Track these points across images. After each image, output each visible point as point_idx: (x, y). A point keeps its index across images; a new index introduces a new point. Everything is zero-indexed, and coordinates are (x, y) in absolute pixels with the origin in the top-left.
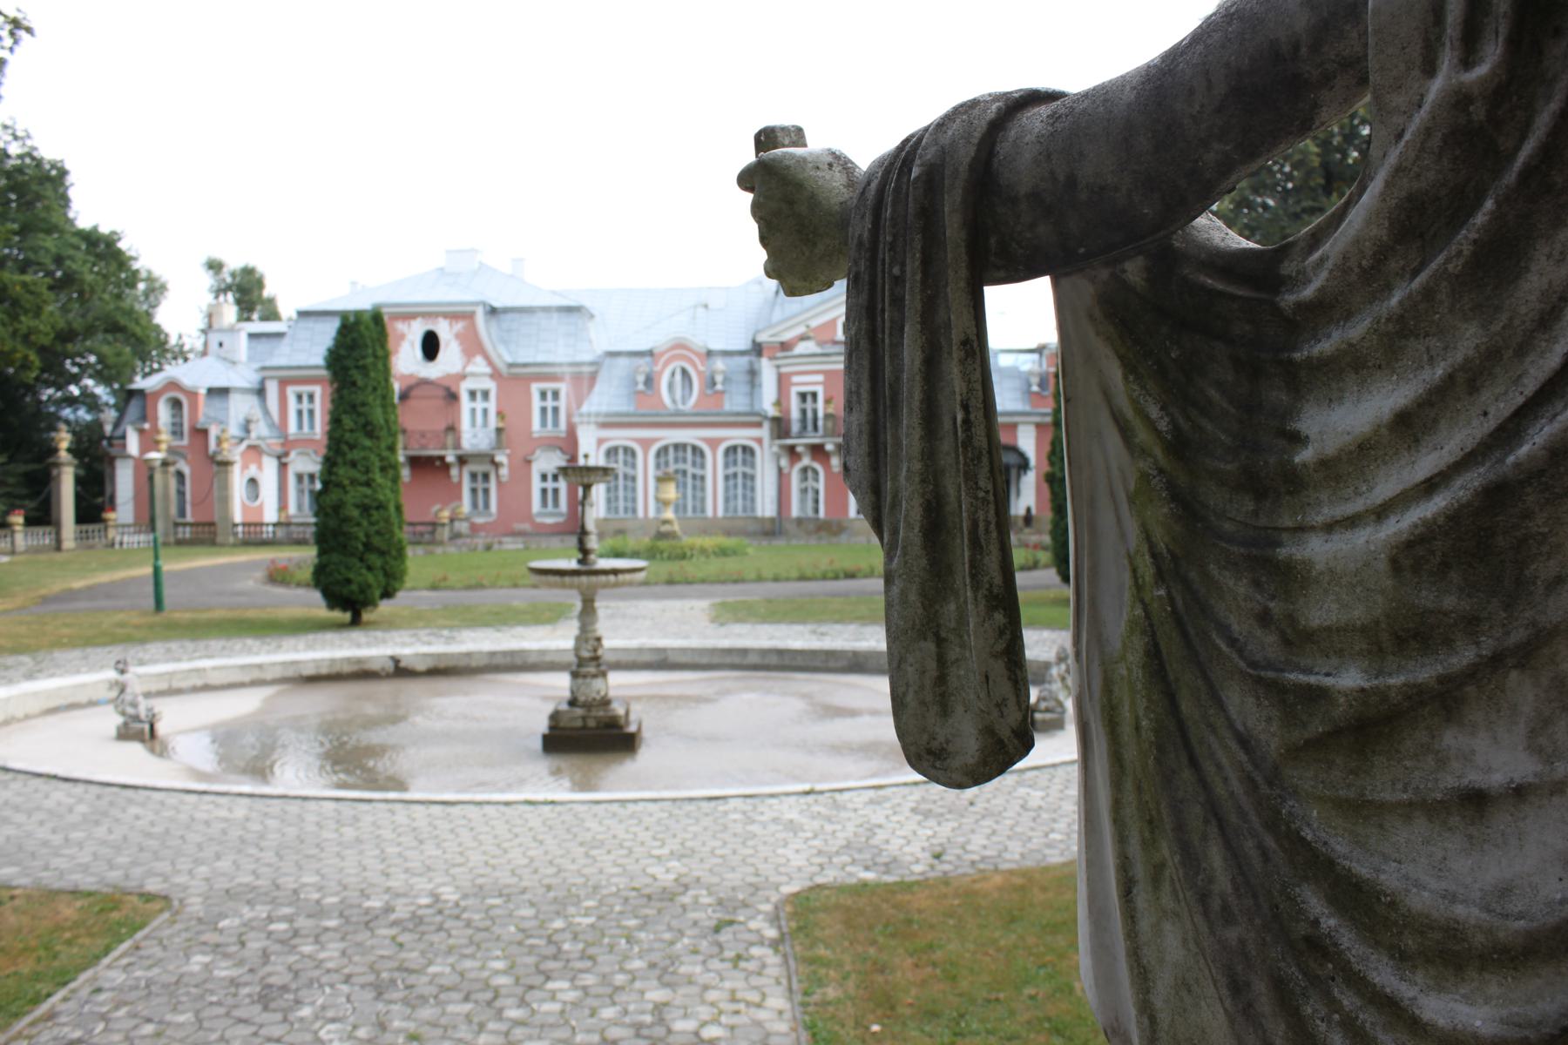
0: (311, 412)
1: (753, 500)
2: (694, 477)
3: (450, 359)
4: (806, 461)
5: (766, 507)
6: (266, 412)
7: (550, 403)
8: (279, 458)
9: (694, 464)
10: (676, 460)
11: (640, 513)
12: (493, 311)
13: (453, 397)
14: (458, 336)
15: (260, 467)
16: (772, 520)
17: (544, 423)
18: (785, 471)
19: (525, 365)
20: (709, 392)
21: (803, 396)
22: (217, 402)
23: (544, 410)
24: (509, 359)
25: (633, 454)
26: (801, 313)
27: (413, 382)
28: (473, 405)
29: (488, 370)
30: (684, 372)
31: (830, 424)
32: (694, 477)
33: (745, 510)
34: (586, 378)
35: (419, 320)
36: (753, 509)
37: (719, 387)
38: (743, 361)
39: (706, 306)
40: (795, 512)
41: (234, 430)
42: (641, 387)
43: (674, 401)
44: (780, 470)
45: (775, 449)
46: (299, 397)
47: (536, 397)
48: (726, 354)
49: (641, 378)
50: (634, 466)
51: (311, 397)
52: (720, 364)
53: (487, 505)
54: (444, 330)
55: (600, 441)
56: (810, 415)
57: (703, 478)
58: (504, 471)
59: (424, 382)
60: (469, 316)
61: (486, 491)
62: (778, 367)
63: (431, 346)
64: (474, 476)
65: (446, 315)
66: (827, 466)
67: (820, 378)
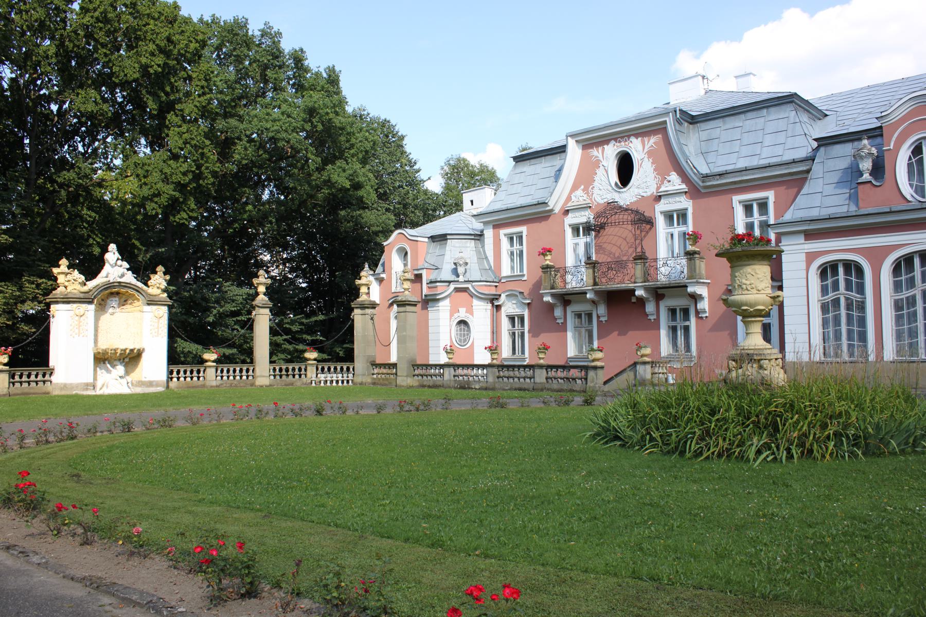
0: (521, 252)
6: (482, 257)
11: (872, 358)
13: (643, 221)
14: (650, 154)
15: (470, 311)
19: (721, 175)
22: (435, 248)
24: (704, 170)
25: (860, 271)
28: (671, 230)
41: (446, 274)
42: (866, 176)
47: (739, 211)
49: (866, 165)
50: (861, 289)
51: (521, 238)
54: (637, 148)
55: (811, 257)
58: (704, 305)
59: (613, 208)
61: (687, 329)
64: (673, 312)
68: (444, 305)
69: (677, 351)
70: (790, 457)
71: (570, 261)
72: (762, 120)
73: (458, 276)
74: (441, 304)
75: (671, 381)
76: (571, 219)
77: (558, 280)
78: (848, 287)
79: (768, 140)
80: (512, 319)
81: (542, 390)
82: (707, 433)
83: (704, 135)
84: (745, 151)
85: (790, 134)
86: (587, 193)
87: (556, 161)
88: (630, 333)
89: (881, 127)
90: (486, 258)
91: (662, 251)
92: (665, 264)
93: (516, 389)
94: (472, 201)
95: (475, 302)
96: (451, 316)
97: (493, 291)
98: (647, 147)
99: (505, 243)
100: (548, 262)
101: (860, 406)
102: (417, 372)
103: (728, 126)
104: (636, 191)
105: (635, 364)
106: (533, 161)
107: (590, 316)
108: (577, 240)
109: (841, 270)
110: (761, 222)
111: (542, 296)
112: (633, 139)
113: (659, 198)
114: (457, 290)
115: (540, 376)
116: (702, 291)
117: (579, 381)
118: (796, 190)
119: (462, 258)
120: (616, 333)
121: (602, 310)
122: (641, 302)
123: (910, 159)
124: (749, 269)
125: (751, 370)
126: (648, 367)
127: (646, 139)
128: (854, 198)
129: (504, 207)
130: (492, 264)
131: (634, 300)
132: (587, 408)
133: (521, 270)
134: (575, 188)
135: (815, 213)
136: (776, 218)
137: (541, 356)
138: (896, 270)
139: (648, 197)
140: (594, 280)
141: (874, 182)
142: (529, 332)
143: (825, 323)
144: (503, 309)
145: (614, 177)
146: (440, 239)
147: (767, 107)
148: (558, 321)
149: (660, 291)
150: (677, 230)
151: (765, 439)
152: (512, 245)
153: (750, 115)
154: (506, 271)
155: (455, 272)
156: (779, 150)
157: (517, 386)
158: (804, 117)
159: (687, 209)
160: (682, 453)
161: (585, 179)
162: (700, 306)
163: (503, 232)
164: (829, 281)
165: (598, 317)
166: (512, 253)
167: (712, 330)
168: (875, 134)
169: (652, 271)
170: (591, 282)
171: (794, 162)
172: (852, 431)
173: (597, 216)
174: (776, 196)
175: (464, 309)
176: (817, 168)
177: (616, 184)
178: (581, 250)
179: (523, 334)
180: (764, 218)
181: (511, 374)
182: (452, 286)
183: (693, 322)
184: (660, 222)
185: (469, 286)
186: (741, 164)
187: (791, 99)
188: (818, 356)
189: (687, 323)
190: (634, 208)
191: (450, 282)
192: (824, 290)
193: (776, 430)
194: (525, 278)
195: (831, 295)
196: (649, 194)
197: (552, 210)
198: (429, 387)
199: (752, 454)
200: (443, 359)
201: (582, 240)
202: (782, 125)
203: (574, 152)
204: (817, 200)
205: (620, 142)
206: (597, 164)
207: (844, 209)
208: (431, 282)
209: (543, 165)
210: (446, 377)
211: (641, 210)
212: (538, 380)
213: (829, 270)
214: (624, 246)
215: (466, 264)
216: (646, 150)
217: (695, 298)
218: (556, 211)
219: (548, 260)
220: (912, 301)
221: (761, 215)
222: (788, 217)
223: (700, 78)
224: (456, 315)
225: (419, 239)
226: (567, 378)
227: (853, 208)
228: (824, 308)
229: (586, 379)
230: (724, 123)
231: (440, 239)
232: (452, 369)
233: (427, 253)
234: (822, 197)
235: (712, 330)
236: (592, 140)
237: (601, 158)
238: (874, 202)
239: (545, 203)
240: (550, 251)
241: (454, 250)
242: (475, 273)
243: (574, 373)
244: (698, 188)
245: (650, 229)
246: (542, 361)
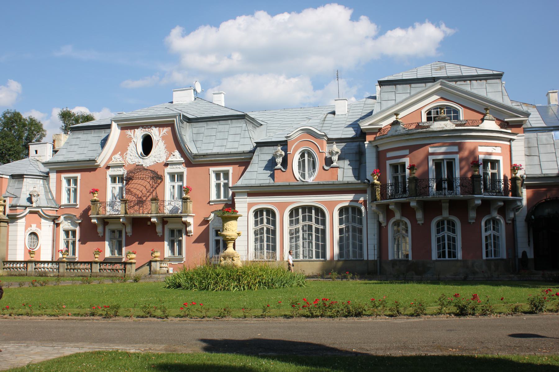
0: (75, 190)
1: (361, 248)
2: (317, 230)
3: (160, 152)
4: (398, 216)
5: (370, 253)
7: (222, 181)
8: (53, 221)
9: (317, 222)
10: (304, 219)
11: (278, 259)
12: (190, 121)
13: (158, 178)
14: (163, 138)
15: (39, 226)
16: (374, 261)
17: (218, 195)
18: (383, 225)
19: (204, 155)
20: (326, 168)
21: (395, 167)
22: (15, 183)
23: (218, 186)
24: (194, 151)
26: (392, 107)
27: (131, 168)
29: (182, 159)
30: (310, 154)
31: (413, 186)
32: (317, 230)
33: (354, 252)
34: (243, 161)
35: (139, 130)
36: (361, 255)
37: (335, 164)
38: (354, 145)
39: (334, 113)
40: (390, 258)
42: (279, 166)
43: (303, 175)
44: (380, 224)
45: (374, 208)
46: (69, 181)
47: (213, 176)
48: (339, 141)
49: (279, 160)
50: (274, 224)
52: (336, 148)
53: (180, 253)
54: (155, 133)
55: (250, 205)
56: (400, 180)
57: (324, 231)
58: (190, 228)
59: (140, 168)
60: (171, 125)
61: (180, 242)
62: (377, 147)
63: (148, 145)
65: (156, 126)
66: (414, 221)
67: (406, 152)
68: (21, 222)
69: (174, 254)
70: (244, 289)
71: (109, 198)
72: (228, 126)
73: (32, 203)
74: (19, 221)
75: (171, 271)
76: (111, 172)
77: (101, 209)
78: (268, 223)
79: (231, 138)
80: (67, 232)
81: (96, 276)
82: (216, 283)
83: (195, 130)
84: (218, 143)
85: (242, 136)
86: (123, 157)
87: (103, 134)
88: (146, 243)
89: (286, 141)
90: (50, 192)
91: (168, 197)
92: (170, 204)
93: (79, 276)
94: (36, 151)
95: (43, 221)
96: (26, 229)
97: (54, 214)
98: (161, 134)
99: (64, 183)
100: (95, 198)
101: (267, 273)
102: (6, 266)
103: (209, 127)
104: (154, 159)
105: (151, 262)
106: (85, 131)
107: (120, 232)
108: (114, 185)
109: (265, 213)
110: (224, 183)
111: (91, 219)
112: (154, 129)
113: (166, 165)
114: (31, 212)
115: (96, 268)
116: (190, 220)
117: (120, 271)
118: (244, 167)
119: (35, 191)
120: (137, 243)
121: (129, 229)
122: (154, 224)
123: (299, 159)
124: (229, 223)
125: (229, 261)
126: (158, 263)
127: (161, 129)
128: (272, 176)
129: (66, 160)
130: (55, 196)
131: (149, 223)
132: (135, 284)
133: (75, 200)
134: (114, 153)
135: (253, 183)
136: (232, 184)
137: (97, 256)
138: (291, 215)
139: (160, 163)
140: (126, 211)
141: (283, 169)
142: (79, 241)
143: (256, 240)
144: (61, 225)
145: (140, 150)
146: (20, 177)
147: (231, 119)
148: (99, 235)
149: (165, 219)
150: (177, 184)
151: (236, 283)
152: (69, 184)
153: (222, 122)
154: (64, 201)
155: (30, 200)
156: (236, 145)
157: (80, 274)
158: (250, 127)
159: (183, 173)
160: (208, 289)
161: (122, 148)
162: (188, 229)
163: (63, 176)
164: (259, 219)
165: (126, 233)
166: (69, 190)
167: (195, 242)
168: (284, 144)
169: (161, 208)
170: (123, 211)
171: (244, 153)
172: (264, 281)
173: (129, 172)
174: (233, 170)
175: (35, 225)
176: (255, 158)
177: (141, 154)
178: (117, 192)
179: (74, 243)
180: (226, 181)
181: (72, 267)
182: (28, 210)
183: (184, 238)
184: (167, 178)
185: (39, 210)
186: (216, 150)
187: (242, 117)
188: (251, 257)
189: (180, 238)
190: (153, 169)
191: (26, 207)
192: (256, 223)
193: (239, 281)
194: (78, 207)
195: (260, 226)
196: (161, 161)
197: (99, 165)
198: (16, 275)
199: (232, 289)
200: (21, 258)
201: (118, 185)
202: (238, 130)
203: (115, 131)
204: (254, 175)
205: (145, 128)
206: (130, 140)
207: (268, 182)
208: (12, 206)
209: (92, 135)
210: (29, 268)
211: (156, 171)
212: (94, 270)
213: (258, 213)
214: (144, 191)
215: (38, 195)
216: (161, 136)
217: (186, 224)
218: (102, 166)
219: (96, 197)
220: (297, 231)
221: (225, 179)
222: (240, 183)
223: (192, 90)
224: (29, 229)
225: (4, 176)
226: (113, 269)
227: (272, 181)
228: (256, 233)
229: (125, 270)
230: (207, 125)
231: (20, 177)
232: (34, 264)
233: (8, 186)
234: (257, 175)
235: (195, 242)
236: (127, 126)
237: (133, 137)
238: (282, 179)
239: (94, 161)
240: (97, 191)
241: (30, 186)
242: (44, 203)
243: (118, 266)
244: (191, 161)
245: (161, 182)
246: (97, 259)
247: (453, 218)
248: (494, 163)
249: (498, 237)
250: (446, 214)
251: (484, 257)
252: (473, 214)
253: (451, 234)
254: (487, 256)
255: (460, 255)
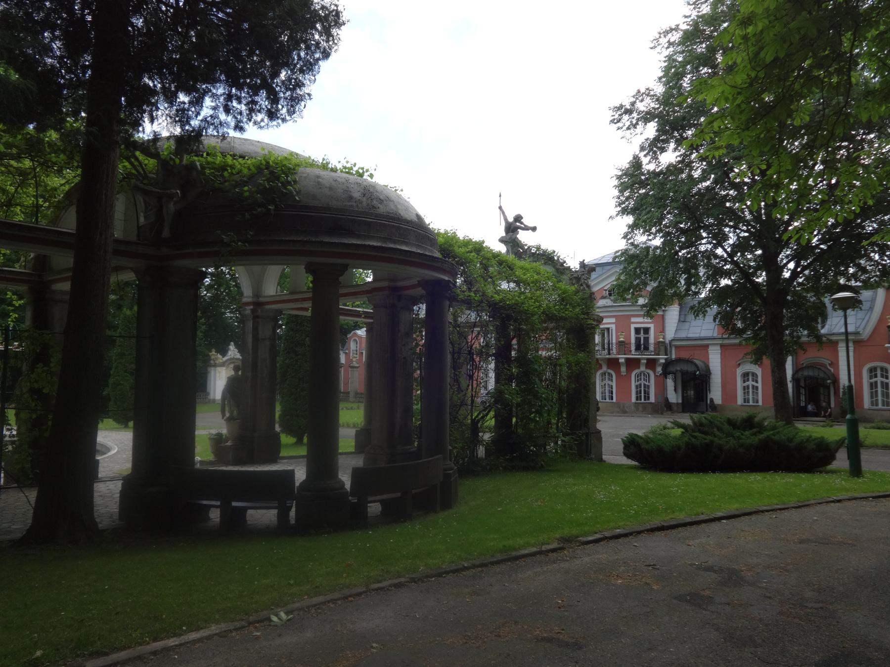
247: (610, 371)
248: (647, 330)
249: (648, 386)
250: (604, 368)
251: (634, 400)
252: (623, 369)
253: (610, 383)
254: (637, 399)
255: (614, 400)
